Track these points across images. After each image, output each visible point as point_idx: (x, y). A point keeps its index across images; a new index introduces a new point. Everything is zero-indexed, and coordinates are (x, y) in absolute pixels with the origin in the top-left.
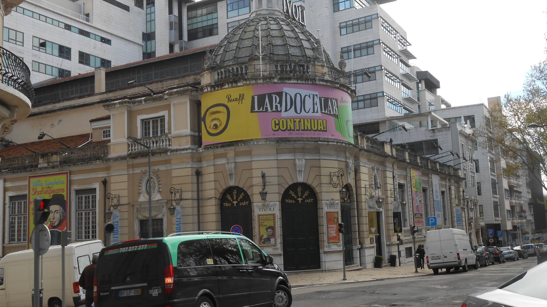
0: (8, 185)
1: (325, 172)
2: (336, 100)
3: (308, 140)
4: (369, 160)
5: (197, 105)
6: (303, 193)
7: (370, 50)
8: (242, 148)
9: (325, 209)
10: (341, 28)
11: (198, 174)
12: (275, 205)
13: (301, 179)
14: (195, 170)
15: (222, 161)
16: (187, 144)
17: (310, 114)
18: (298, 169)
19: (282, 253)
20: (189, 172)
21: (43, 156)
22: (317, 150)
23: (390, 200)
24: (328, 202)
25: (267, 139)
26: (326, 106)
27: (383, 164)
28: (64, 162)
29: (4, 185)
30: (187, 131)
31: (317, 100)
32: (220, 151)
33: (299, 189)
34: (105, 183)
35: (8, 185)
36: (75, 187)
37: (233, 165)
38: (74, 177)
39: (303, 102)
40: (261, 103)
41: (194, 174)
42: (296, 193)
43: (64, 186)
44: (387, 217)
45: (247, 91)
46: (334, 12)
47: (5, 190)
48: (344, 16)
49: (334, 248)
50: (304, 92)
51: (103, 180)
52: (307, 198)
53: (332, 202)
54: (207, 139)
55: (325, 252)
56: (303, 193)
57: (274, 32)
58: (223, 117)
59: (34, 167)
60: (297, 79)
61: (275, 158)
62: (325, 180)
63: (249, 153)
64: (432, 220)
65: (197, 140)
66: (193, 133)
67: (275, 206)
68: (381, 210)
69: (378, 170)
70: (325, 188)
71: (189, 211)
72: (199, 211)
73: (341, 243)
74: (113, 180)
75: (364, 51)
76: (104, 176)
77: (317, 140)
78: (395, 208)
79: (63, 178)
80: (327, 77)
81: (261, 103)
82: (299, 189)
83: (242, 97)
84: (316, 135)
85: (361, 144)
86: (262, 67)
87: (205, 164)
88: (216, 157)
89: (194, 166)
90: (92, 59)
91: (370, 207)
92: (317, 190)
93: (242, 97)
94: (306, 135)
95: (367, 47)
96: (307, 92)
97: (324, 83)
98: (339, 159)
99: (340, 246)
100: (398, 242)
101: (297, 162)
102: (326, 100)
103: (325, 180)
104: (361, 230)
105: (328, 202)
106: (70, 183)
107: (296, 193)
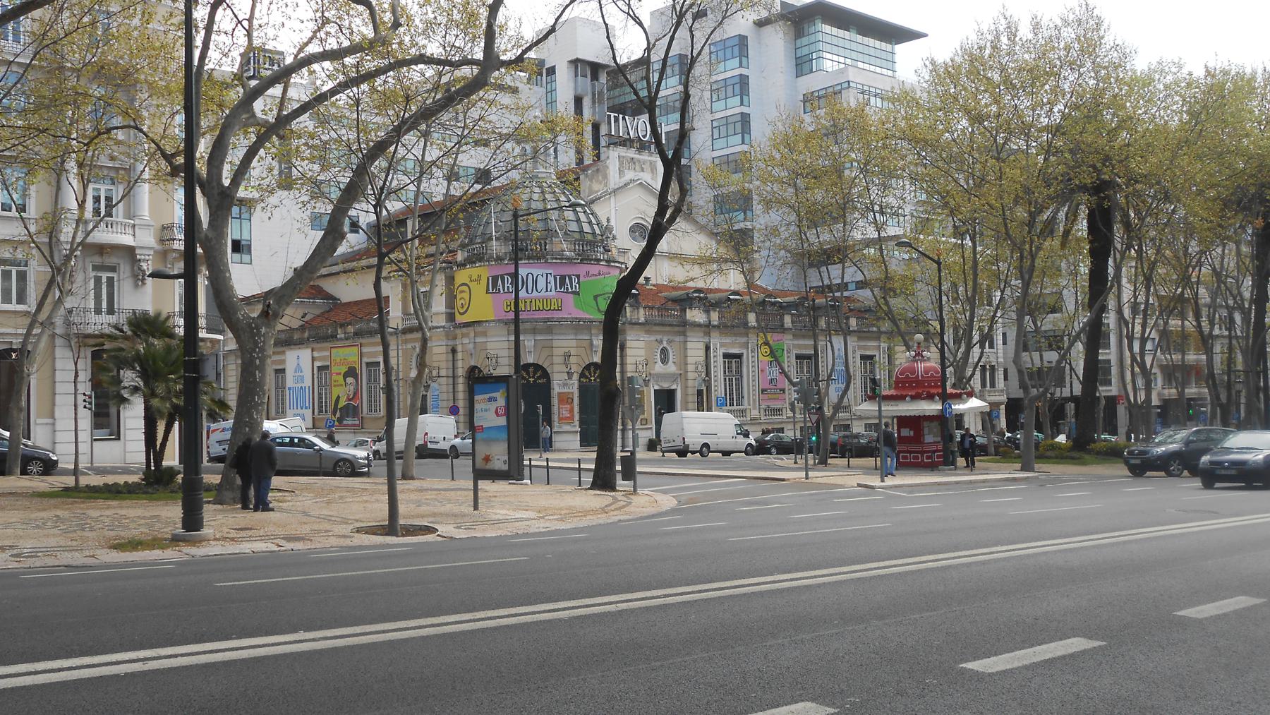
0: (316, 354)
1: (556, 352)
2: (578, 276)
3: (536, 320)
4: (648, 332)
5: (450, 280)
6: (535, 373)
8: (479, 329)
9: (556, 389)
10: (804, 102)
11: (454, 351)
15: (466, 341)
16: (441, 321)
17: (543, 293)
20: (443, 349)
21: (342, 326)
22: (549, 330)
23: (691, 375)
25: (499, 321)
26: (562, 283)
27: (684, 334)
28: (358, 334)
30: (443, 309)
31: (551, 279)
32: (465, 330)
33: (531, 370)
35: (316, 354)
36: (365, 360)
37: (471, 346)
38: (365, 350)
39: (535, 282)
40: (495, 285)
42: (528, 373)
43: (356, 358)
44: (685, 395)
45: (482, 272)
47: (313, 359)
48: (812, 83)
49: (566, 428)
50: (536, 272)
52: (539, 378)
54: (460, 319)
56: (535, 373)
58: (466, 296)
59: (334, 337)
60: (529, 258)
62: (557, 360)
63: (484, 334)
65: (451, 317)
68: (674, 387)
69: (669, 342)
70: (556, 368)
71: (444, 388)
73: (577, 423)
77: (548, 320)
79: (355, 350)
81: (495, 285)
82: (531, 370)
83: (480, 276)
84: (549, 315)
86: (496, 247)
87: (458, 341)
88: (463, 336)
93: (480, 276)
94: (537, 315)
96: (539, 271)
102: (563, 278)
106: (361, 355)
107: (528, 373)
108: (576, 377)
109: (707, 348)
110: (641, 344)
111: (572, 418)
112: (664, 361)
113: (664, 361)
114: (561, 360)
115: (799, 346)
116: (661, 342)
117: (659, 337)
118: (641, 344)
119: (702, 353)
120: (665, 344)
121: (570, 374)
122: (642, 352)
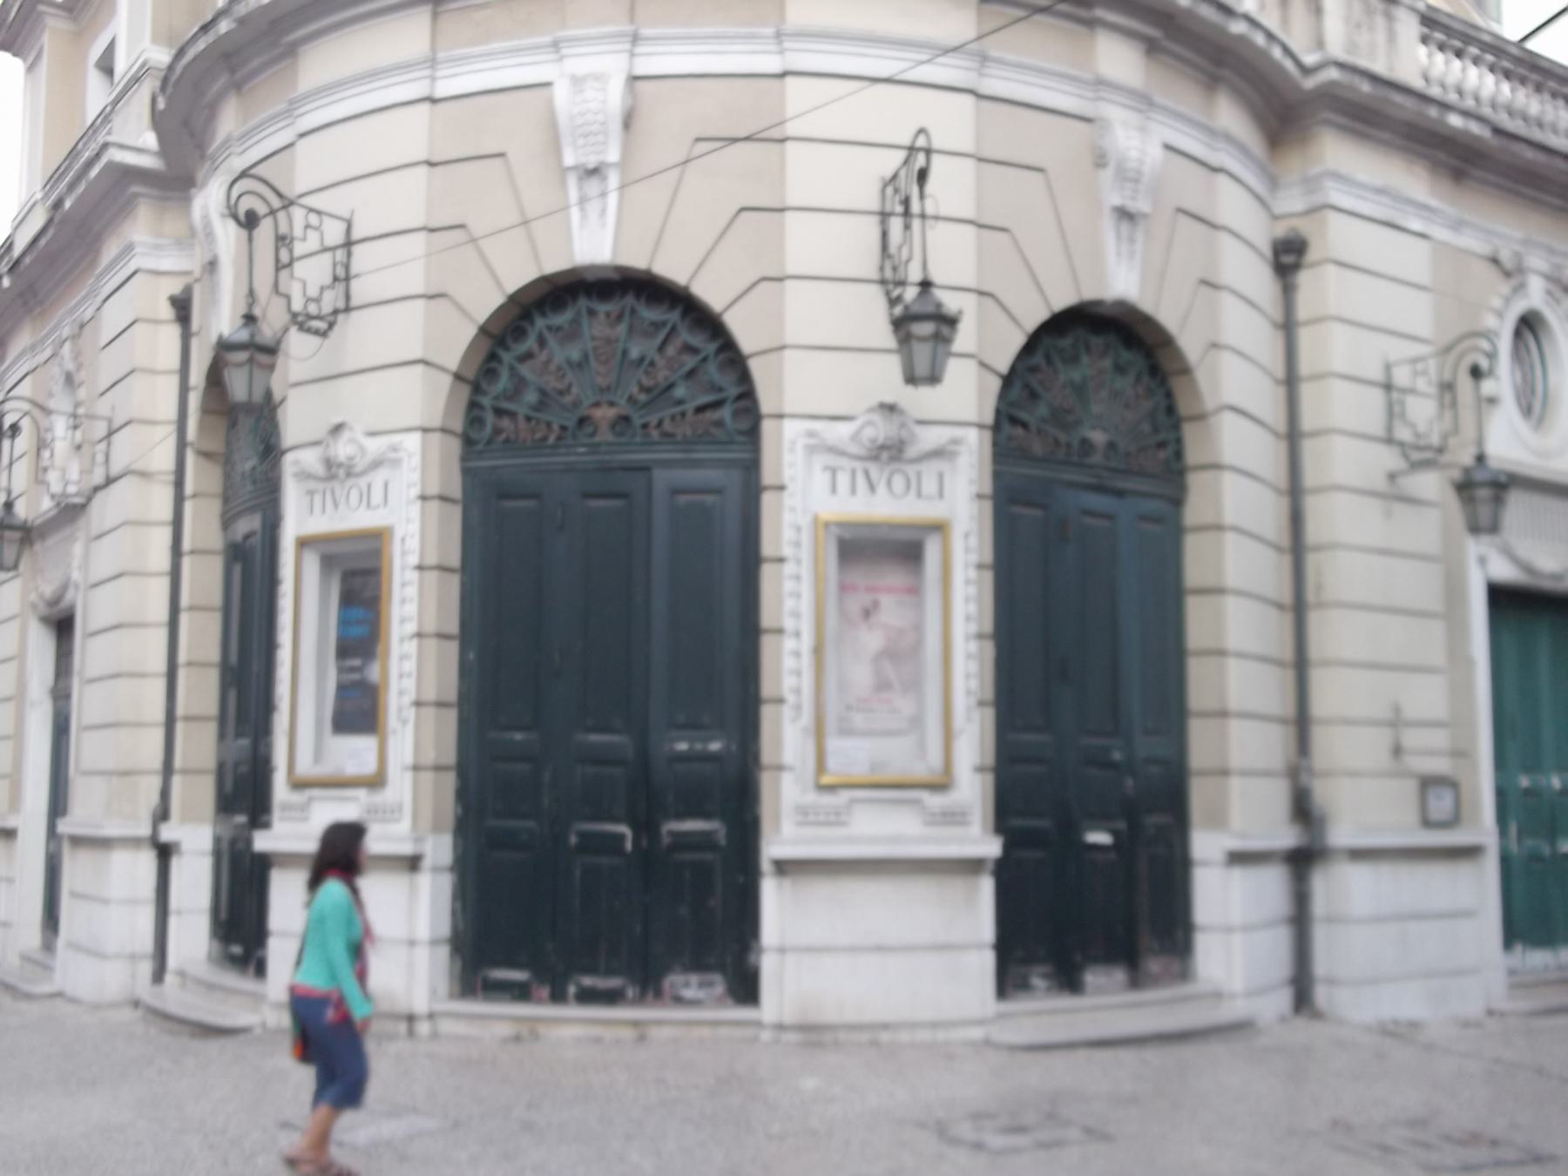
1: (809, 174)
9: (807, 492)
13: (593, 243)
14: (175, 287)
18: (569, 159)
19: (440, 849)
24: (840, 433)
41: (167, 312)
53: (881, 430)
55: (783, 867)
67: (396, 463)
85: (1352, 46)
89: (166, 264)
92: (745, 330)
98: (996, 84)
99: (953, 817)
101: (561, 95)
105: (840, 433)
108: (965, 394)
110: (1410, 258)
112: (1534, 403)
113: (1534, 403)
114: (855, 246)
120: (1535, 295)
121: (921, 327)
122: (1417, 314)
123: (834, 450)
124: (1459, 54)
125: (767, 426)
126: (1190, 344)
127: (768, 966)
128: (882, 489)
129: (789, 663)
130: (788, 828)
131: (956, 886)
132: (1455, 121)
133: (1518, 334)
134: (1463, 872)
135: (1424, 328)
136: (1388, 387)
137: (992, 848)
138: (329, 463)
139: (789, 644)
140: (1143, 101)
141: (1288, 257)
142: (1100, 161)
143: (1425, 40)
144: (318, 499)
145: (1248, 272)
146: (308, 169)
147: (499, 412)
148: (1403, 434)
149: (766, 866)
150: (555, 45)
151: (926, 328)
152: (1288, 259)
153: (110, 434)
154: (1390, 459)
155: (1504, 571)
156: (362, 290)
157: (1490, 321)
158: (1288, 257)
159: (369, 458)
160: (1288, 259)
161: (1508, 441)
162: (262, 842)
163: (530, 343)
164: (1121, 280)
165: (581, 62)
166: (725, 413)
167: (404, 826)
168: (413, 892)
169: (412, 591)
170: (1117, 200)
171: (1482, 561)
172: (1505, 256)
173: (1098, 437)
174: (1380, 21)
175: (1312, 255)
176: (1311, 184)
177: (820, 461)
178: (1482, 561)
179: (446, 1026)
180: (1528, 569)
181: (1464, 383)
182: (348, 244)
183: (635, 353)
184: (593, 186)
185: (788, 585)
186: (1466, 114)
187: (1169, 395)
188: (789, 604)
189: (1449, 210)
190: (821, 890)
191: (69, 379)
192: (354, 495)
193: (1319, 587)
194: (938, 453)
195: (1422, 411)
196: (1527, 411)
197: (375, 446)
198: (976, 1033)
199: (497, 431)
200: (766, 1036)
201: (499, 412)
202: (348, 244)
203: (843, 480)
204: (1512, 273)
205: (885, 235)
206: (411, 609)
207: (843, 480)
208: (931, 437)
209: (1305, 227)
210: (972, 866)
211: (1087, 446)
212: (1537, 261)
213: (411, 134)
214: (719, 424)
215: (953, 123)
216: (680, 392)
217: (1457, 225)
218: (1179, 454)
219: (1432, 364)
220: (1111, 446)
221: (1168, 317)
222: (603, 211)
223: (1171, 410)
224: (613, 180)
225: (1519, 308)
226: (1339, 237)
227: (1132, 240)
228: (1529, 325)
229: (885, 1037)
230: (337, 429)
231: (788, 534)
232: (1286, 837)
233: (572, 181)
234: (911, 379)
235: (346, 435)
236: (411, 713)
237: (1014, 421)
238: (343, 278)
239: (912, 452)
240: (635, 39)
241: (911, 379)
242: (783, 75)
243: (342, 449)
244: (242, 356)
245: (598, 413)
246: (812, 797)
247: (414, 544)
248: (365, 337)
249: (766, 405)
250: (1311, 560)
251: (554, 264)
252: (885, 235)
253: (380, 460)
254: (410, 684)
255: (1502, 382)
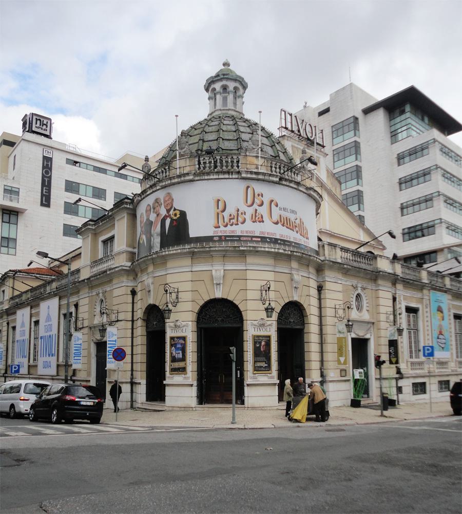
1: (250, 285)
7: (427, 177)
9: (250, 332)
12: (187, 326)
13: (219, 294)
14: (131, 289)
18: (215, 282)
19: (195, 383)
23: (383, 325)
24: (255, 323)
29: (31, 311)
34: (76, 306)
41: (130, 293)
44: (378, 345)
46: (392, 144)
51: (75, 303)
53: (262, 322)
55: (248, 385)
57: (210, 128)
61: (190, 270)
62: (251, 295)
64: (428, 350)
66: (130, 249)
67: (187, 326)
68: (367, 336)
69: (364, 289)
72: (132, 333)
74: (80, 304)
75: (421, 179)
76: (75, 300)
78: (392, 335)
80: (262, 170)
85: (329, 255)
89: (129, 285)
90: (82, 188)
91: (340, 332)
92: (241, 308)
95: (425, 175)
97: (254, 176)
98: (277, 270)
99: (272, 377)
100: (397, 376)
101: (214, 272)
103: (253, 295)
104: (325, 359)
105: (255, 323)
108: (275, 316)
109: (394, 299)
110: (339, 287)
111: (269, 368)
112: (359, 308)
113: (359, 308)
114: (257, 295)
115: (455, 307)
116: (355, 288)
117: (354, 282)
118: (339, 287)
119: (390, 303)
120: (359, 291)
121: (269, 311)
123: (255, 325)
124: (347, 252)
125: (245, 322)
126: (305, 306)
127: (246, 399)
128: (261, 330)
129: (249, 356)
130: (249, 380)
131: (273, 387)
132: (345, 266)
133: (357, 296)
134: (347, 383)
135: (341, 298)
136: (335, 308)
137: (278, 382)
138: (175, 326)
139: (249, 353)
140: (298, 270)
141: (320, 289)
142: (292, 280)
143: (341, 251)
144: (173, 331)
145: (314, 292)
146: (169, 279)
147: (203, 319)
148: (337, 316)
149: (245, 385)
150: (212, 265)
151: (270, 310)
152: (320, 289)
153: (118, 313)
154: (336, 320)
155: (354, 336)
156: (180, 300)
157: (352, 296)
158: (320, 289)
159: (183, 325)
160: (320, 289)
161: (354, 314)
162: (165, 382)
163: (208, 308)
164: (296, 298)
165: (216, 267)
166: (238, 319)
167: (191, 379)
168: (192, 389)
169: (191, 345)
170: (294, 286)
171: (350, 334)
172: (354, 285)
173: (292, 320)
174: (334, 250)
175: (323, 289)
176: (324, 278)
177: (253, 326)
178: (350, 334)
179: (197, 409)
180: (358, 335)
181: (347, 309)
182: (178, 292)
183: (224, 310)
184: (218, 286)
185: (249, 345)
186: (347, 265)
187: (302, 313)
188: (249, 347)
189: (345, 279)
190: (254, 388)
191: (102, 301)
192: (180, 330)
193: (325, 340)
194: (269, 325)
195: (341, 312)
196: (358, 309)
197: (184, 323)
198: (276, 408)
199: (203, 321)
200: (246, 409)
201: (203, 319)
202: (178, 292)
203: (256, 329)
204: (355, 288)
205: (262, 293)
206: (191, 348)
207: (256, 329)
208: (269, 323)
209: (322, 283)
210: (275, 384)
211: (290, 322)
212: (360, 285)
213: (189, 276)
214: (237, 321)
215: (270, 276)
216: (231, 316)
217: (346, 281)
218: (304, 322)
219: (342, 305)
220: (294, 321)
221: (302, 302)
222: (220, 290)
223: (302, 315)
224: (221, 286)
225: (357, 293)
226: (328, 286)
227: (297, 291)
228: (358, 296)
229: (263, 408)
230: (177, 320)
231: (248, 337)
232: (320, 379)
233: (215, 286)
234: (268, 317)
235: (179, 321)
236: (191, 363)
237: (280, 319)
238: (177, 298)
239: (266, 325)
240: (224, 264)
241: (268, 317)
242: (246, 270)
243: (178, 324)
244: (167, 312)
245: (219, 319)
246: (252, 375)
247: (191, 338)
248: (180, 307)
249: (244, 318)
250: (323, 336)
251: (212, 297)
252: (262, 293)
253: (183, 325)
254: (191, 359)
255: (354, 304)
